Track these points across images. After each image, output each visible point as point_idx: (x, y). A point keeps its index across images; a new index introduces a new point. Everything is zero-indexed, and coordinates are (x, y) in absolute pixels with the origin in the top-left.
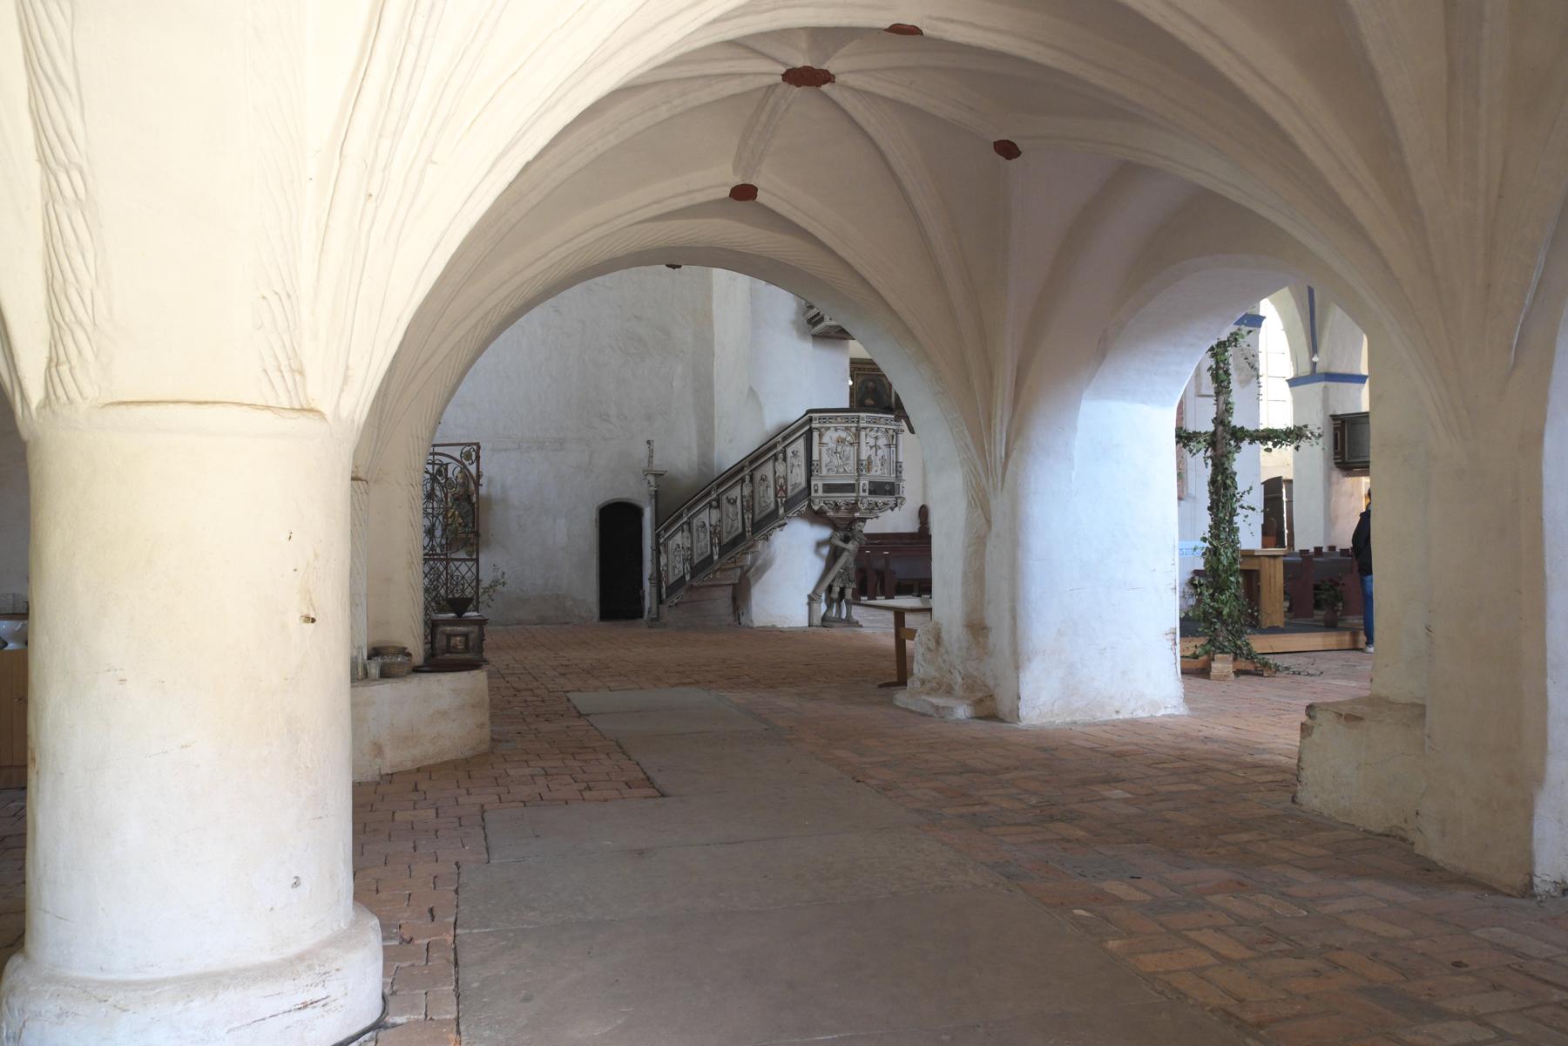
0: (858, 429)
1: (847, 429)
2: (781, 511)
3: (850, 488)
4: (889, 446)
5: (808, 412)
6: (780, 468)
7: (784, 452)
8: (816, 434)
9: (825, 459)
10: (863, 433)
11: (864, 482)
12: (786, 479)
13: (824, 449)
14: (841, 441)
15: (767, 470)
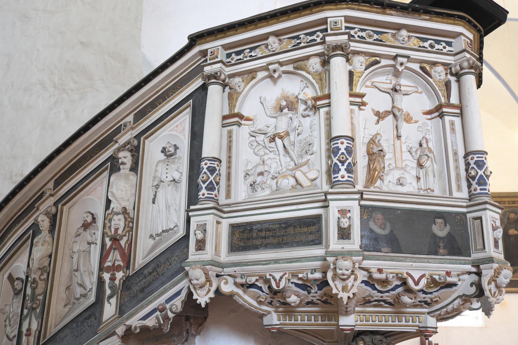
0: (326, 63)
1: (299, 64)
2: (109, 309)
3: (307, 230)
4: (438, 112)
5: (195, 39)
6: (122, 188)
7: (136, 151)
8: (214, 92)
9: (245, 156)
10: (338, 63)
11: (343, 210)
12: (132, 222)
13: (242, 134)
14: (289, 105)
15: (93, 200)
